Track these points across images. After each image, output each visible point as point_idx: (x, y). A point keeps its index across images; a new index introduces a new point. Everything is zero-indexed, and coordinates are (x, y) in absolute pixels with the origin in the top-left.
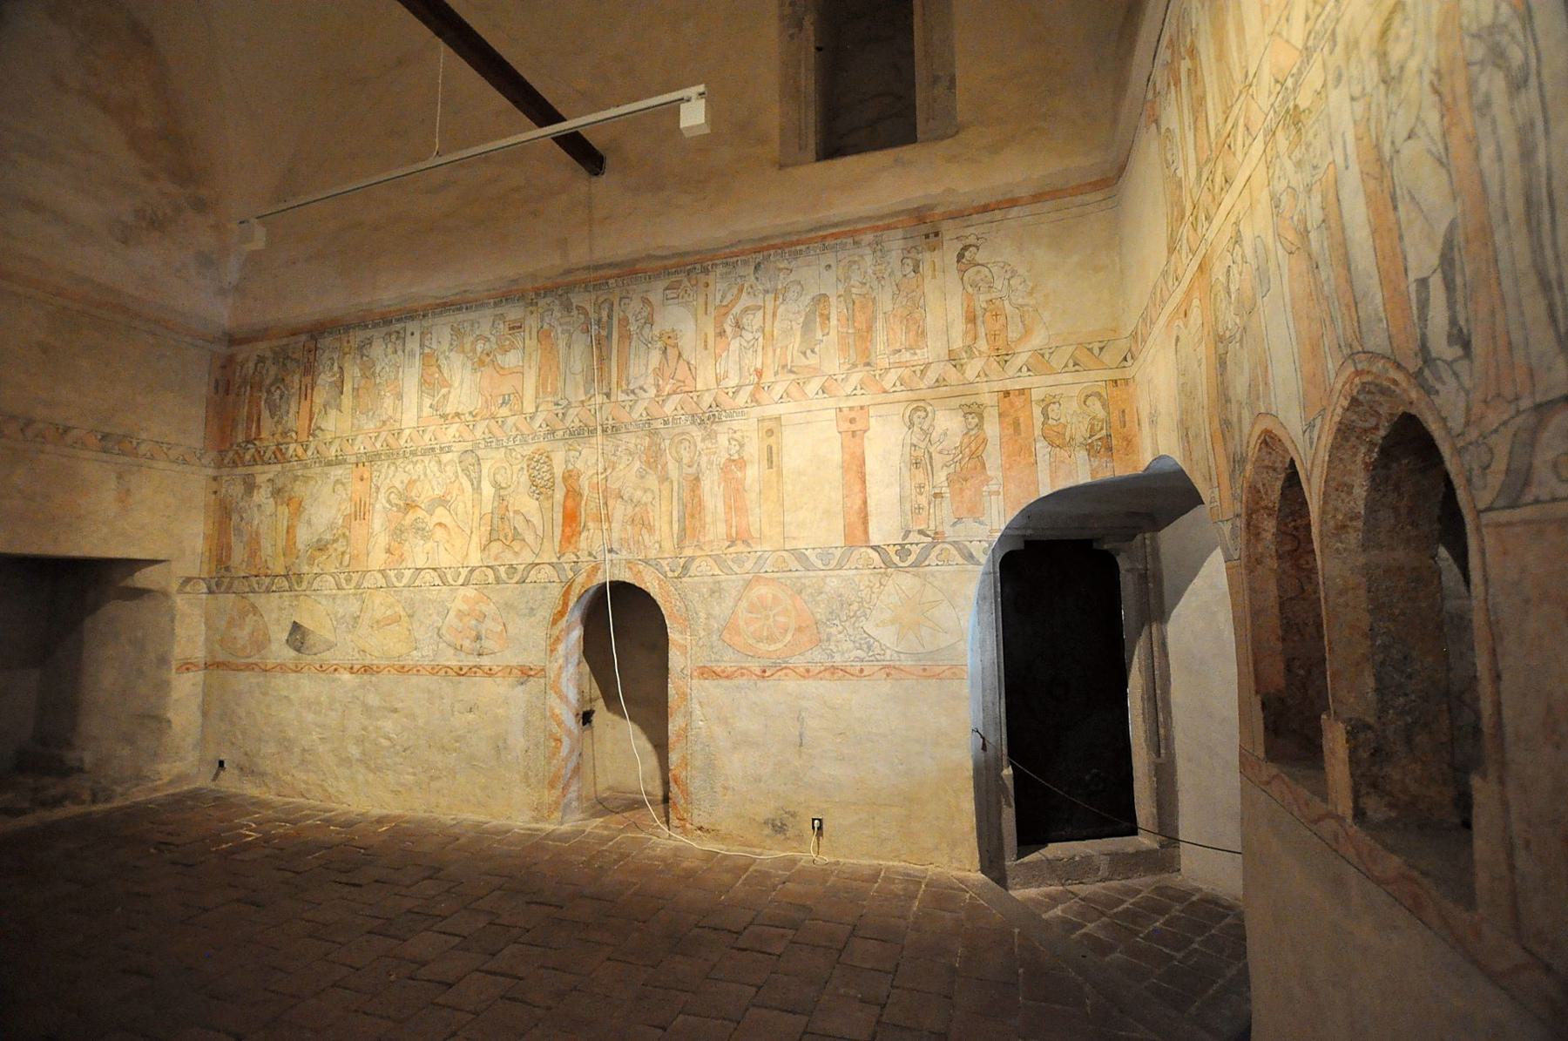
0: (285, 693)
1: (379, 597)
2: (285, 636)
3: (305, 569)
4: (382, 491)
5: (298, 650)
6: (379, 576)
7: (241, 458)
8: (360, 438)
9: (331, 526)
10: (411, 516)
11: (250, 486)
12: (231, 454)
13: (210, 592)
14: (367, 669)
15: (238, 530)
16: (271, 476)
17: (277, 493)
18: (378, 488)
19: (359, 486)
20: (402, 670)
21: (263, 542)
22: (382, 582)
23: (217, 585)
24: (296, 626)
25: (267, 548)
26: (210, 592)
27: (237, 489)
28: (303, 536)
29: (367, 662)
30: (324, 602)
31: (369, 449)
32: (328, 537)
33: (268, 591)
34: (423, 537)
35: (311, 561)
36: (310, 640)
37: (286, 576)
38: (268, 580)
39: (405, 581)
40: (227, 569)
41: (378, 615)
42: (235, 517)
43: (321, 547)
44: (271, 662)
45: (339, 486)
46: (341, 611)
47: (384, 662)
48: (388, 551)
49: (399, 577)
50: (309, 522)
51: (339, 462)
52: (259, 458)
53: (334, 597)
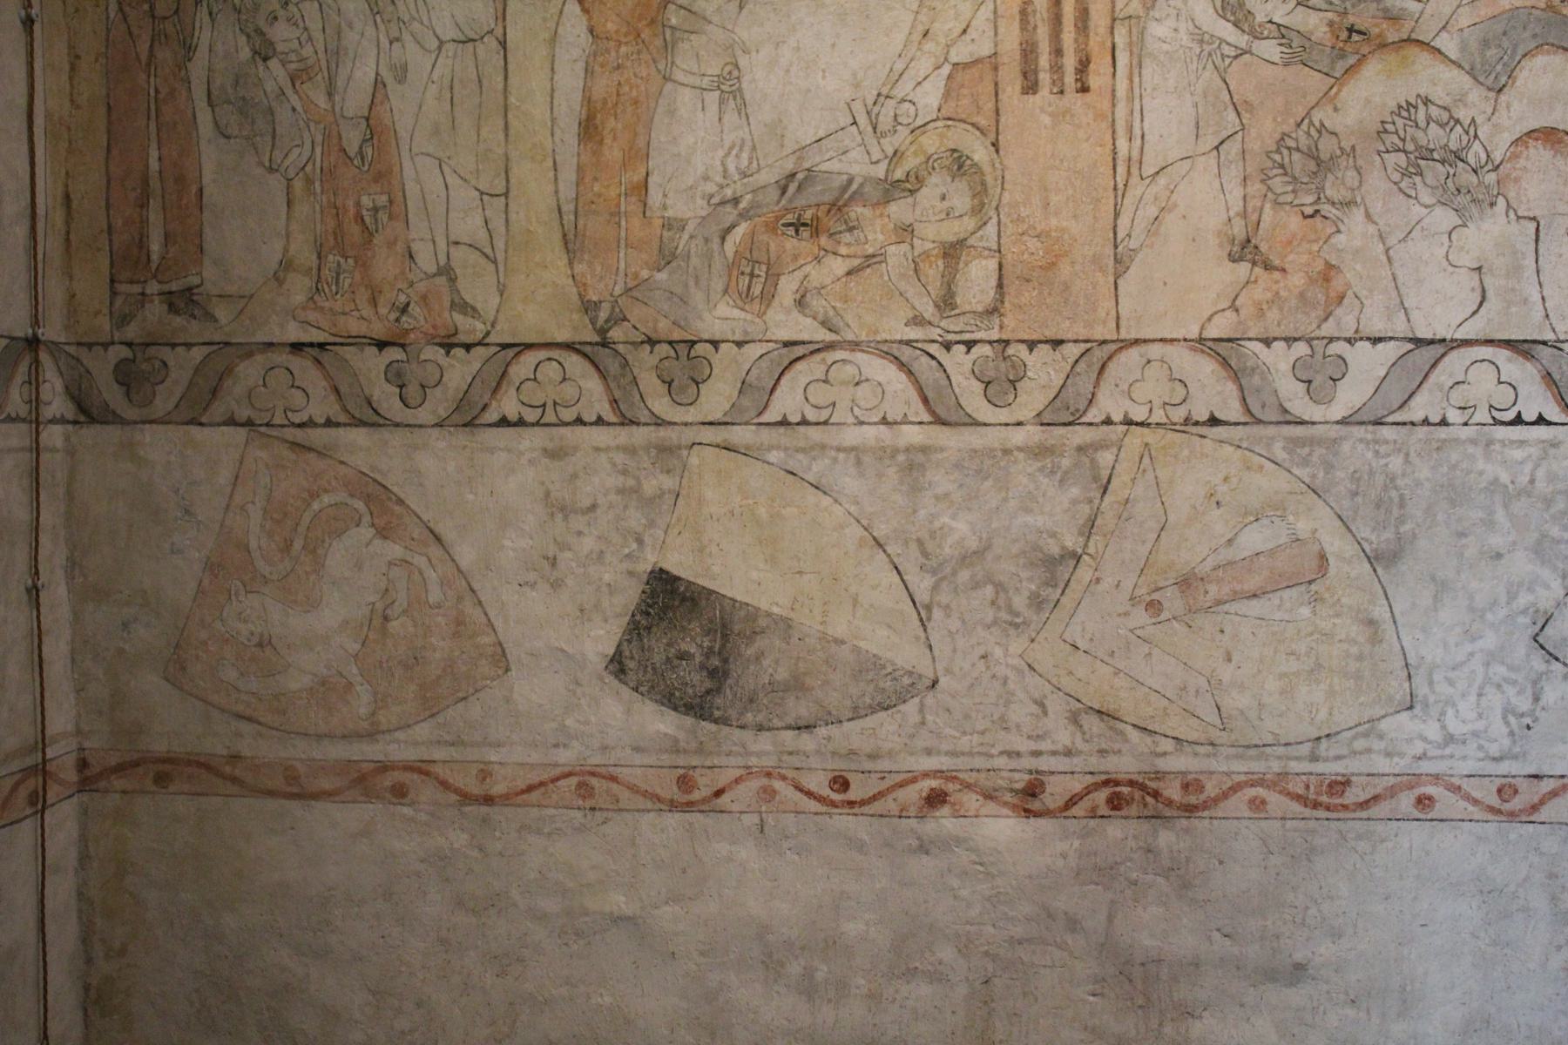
0: (618, 901)
1: (1199, 471)
2: (602, 638)
3: (720, 316)
5: (697, 708)
6: (1203, 369)
9: (872, 114)
10: (1372, 91)
13: (87, 412)
14: (1123, 795)
20: (1329, 799)
21: (419, 176)
22: (1211, 390)
23: (126, 376)
24: (667, 598)
25: (442, 201)
26: (87, 412)
28: (695, 154)
29: (1124, 765)
30: (849, 482)
32: (857, 162)
33: (467, 416)
34: (1450, 195)
35: (754, 279)
36: (767, 663)
37: (596, 350)
38: (459, 371)
39: (1349, 396)
40: (185, 301)
41: (1194, 552)
43: (811, 211)
44: (514, 759)
46: (961, 529)
47: (1227, 765)
48: (1245, 250)
49: (1321, 376)
50: (729, 88)
53: (914, 463)
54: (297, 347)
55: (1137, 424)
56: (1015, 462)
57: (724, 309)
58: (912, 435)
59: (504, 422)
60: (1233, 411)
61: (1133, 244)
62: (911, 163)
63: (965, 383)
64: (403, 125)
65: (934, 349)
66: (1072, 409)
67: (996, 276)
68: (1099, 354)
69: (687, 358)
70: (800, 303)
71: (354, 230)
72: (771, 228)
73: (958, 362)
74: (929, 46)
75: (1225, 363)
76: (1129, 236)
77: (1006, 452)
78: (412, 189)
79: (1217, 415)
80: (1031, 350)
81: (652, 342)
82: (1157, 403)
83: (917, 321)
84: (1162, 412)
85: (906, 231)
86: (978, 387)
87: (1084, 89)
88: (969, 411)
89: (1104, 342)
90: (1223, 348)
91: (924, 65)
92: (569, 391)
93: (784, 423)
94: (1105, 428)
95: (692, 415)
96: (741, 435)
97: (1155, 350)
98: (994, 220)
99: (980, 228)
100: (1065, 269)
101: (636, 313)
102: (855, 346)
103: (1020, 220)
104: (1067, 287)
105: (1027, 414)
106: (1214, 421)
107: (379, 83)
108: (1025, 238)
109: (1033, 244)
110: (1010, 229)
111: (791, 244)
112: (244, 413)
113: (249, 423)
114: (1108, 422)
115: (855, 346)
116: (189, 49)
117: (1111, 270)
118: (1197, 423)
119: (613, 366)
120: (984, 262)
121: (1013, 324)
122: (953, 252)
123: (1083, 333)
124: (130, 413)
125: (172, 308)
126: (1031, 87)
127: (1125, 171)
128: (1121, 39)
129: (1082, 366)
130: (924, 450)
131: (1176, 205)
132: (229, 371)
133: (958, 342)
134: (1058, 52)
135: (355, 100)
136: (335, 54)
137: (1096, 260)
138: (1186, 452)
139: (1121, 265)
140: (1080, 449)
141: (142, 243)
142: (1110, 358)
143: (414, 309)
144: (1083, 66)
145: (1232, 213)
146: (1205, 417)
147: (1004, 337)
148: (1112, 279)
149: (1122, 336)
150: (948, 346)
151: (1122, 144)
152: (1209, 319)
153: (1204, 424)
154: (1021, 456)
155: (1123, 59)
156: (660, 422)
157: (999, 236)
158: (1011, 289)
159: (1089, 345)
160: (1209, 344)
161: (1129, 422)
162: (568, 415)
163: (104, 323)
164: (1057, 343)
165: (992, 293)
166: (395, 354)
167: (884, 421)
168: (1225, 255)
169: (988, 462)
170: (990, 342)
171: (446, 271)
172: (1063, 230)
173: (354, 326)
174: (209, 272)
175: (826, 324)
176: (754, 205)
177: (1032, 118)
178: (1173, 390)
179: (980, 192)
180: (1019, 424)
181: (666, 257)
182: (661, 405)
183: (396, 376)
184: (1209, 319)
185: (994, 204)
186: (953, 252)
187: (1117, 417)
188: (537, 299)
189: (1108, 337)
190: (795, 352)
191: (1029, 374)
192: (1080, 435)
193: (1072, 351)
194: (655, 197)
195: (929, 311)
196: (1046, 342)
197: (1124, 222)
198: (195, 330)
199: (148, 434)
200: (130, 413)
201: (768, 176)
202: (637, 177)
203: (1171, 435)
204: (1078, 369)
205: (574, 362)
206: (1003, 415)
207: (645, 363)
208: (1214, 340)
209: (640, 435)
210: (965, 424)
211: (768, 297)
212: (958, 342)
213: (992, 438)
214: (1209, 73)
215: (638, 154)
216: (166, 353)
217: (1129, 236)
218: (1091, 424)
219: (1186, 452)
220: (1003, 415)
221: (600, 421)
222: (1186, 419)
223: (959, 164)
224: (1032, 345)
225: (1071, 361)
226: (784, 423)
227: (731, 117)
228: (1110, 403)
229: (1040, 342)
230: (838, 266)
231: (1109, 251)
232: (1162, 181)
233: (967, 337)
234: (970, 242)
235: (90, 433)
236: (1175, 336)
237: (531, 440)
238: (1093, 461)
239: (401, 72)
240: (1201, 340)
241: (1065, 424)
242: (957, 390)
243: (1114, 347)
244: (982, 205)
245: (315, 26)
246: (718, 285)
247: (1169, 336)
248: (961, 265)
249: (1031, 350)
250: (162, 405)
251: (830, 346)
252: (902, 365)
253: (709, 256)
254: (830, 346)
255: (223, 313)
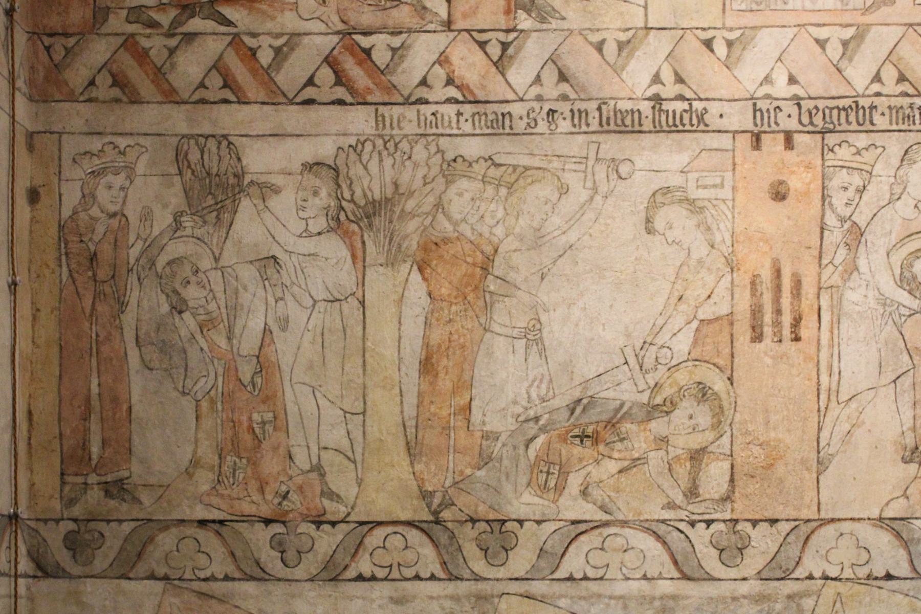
3: (524, 502)
4: (878, 241)
6: (882, 541)
7: (159, 75)
8: (768, 43)
9: (639, 356)
11: (216, 189)
12: (99, 51)
13: (44, 569)
15: (166, 352)
16: (326, 149)
17: (359, 218)
18: (856, 235)
19: (768, 218)
21: (296, 398)
23: (72, 543)
25: (315, 418)
27: (147, 197)
28: (507, 385)
31: (817, 81)
32: (627, 391)
33: (332, 574)
35: (550, 475)
37: (432, 527)
38: (326, 541)
40: (117, 489)
42: (144, 302)
43: (593, 427)
45: (673, 217)
50: (533, 336)
51: (674, 117)
52: (247, 76)
54: (202, 523)
55: (832, 579)
56: (741, 606)
57: (527, 497)
58: (666, 587)
59: (360, 578)
60: (903, 569)
61: (831, 450)
62: (668, 391)
63: (705, 550)
64: (286, 361)
65: (682, 526)
66: (784, 568)
67: (729, 474)
68: (805, 529)
69: (499, 533)
70: (584, 493)
71: (247, 438)
72: (563, 439)
73: (700, 535)
74: (682, 307)
75: (898, 535)
76: (829, 444)
77: (734, 599)
78: (292, 408)
79: (892, 572)
80: (754, 527)
81: (473, 521)
82: (847, 564)
83: (671, 505)
84: (850, 570)
85: (663, 441)
86: (715, 553)
87: (797, 339)
88: (708, 570)
89: (809, 521)
90: (896, 525)
91: (678, 321)
92: (410, 556)
93: (571, 578)
94: (808, 582)
95: (501, 573)
96: (538, 587)
97: (846, 527)
98: (729, 434)
99: (718, 439)
100: (780, 469)
101: (461, 500)
102: (624, 523)
103: (747, 433)
104: (781, 481)
105: (750, 572)
106: (889, 577)
107: (267, 330)
108: (751, 446)
109: (757, 450)
110: (739, 440)
111: (577, 450)
112: (162, 571)
113: (166, 578)
114: (810, 577)
115: (624, 523)
116: (122, 305)
117: (814, 469)
118: (876, 578)
119: (444, 539)
120: (720, 464)
121: (741, 508)
122: (697, 456)
123: (793, 514)
124: (76, 570)
125: (108, 494)
126: (758, 337)
127: (824, 398)
128: (825, 302)
129: (791, 538)
130: (674, 597)
131: (863, 423)
132: (151, 539)
133: (701, 521)
134: (778, 312)
135: (248, 344)
136: (234, 309)
137: (803, 461)
138: (868, 599)
139: (822, 465)
140: (789, 597)
141: (85, 446)
142: (812, 532)
143: (293, 496)
144: (797, 322)
145: (905, 428)
146: (882, 573)
147: (735, 517)
148: (815, 476)
149: (823, 515)
150: (692, 524)
151: (824, 379)
152: (887, 504)
153: (881, 579)
154: (746, 602)
155: (826, 317)
156: (478, 578)
157: (732, 445)
158: (739, 483)
159: (797, 523)
160: (887, 522)
161: (826, 578)
162: (409, 573)
163: (57, 505)
164: (773, 522)
165: (726, 486)
166: (278, 528)
167: (645, 577)
168: (899, 458)
169: (721, 607)
170: (724, 521)
171: (318, 469)
172: (779, 441)
173: (247, 508)
174: (136, 468)
175: (604, 508)
176: (551, 422)
177: (757, 359)
178: (859, 555)
179: (719, 413)
180: (744, 579)
181: (485, 460)
182: (479, 566)
183: (279, 545)
184: (887, 504)
185: (729, 422)
186: (697, 456)
187: (817, 574)
188: (387, 488)
189: (811, 517)
190: (580, 528)
191: (753, 543)
192: (789, 587)
193: (785, 527)
194: (476, 416)
195: (679, 499)
196: (766, 521)
197: (825, 435)
198: (124, 509)
199: (89, 585)
200: (76, 570)
201: (561, 401)
202: (463, 401)
203: (857, 587)
204: (789, 540)
205: (414, 535)
206: (733, 573)
207: (467, 536)
208: (890, 519)
209: (463, 588)
210: (705, 579)
211: (560, 489)
212: (701, 521)
213: (724, 589)
214: (890, 327)
215: (464, 384)
216: (102, 526)
217: (829, 444)
218: (798, 579)
219: (868, 599)
220: (733, 573)
221: (433, 577)
222: (869, 576)
223: (703, 393)
224: (755, 523)
225: (784, 534)
226: (571, 578)
227: (534, 357)
228: (812, 564)
229: (761, 520)
230: (612, 466)
231: (814, 455)
232: (853, 405)
233: (707, 517)
234: (710, 449)
235: (45, 585)
236: (861, 516)
237: (381, 591)
238: (798, 605)
239: (284, 324)
240: (881, 519)
241: (778, 579)
242: (699, 555)
243: (815, 524)
244: (720, 422)
245: (218, 289)
246: (524, 480)
247: (857, 516)
248: (703, 465)
249: (754, 527)
250: (100, 563)
251: (606, 524)
252: (658, 537)
253: (516, 460)
254: (606, 524)
255: (146, 498)
